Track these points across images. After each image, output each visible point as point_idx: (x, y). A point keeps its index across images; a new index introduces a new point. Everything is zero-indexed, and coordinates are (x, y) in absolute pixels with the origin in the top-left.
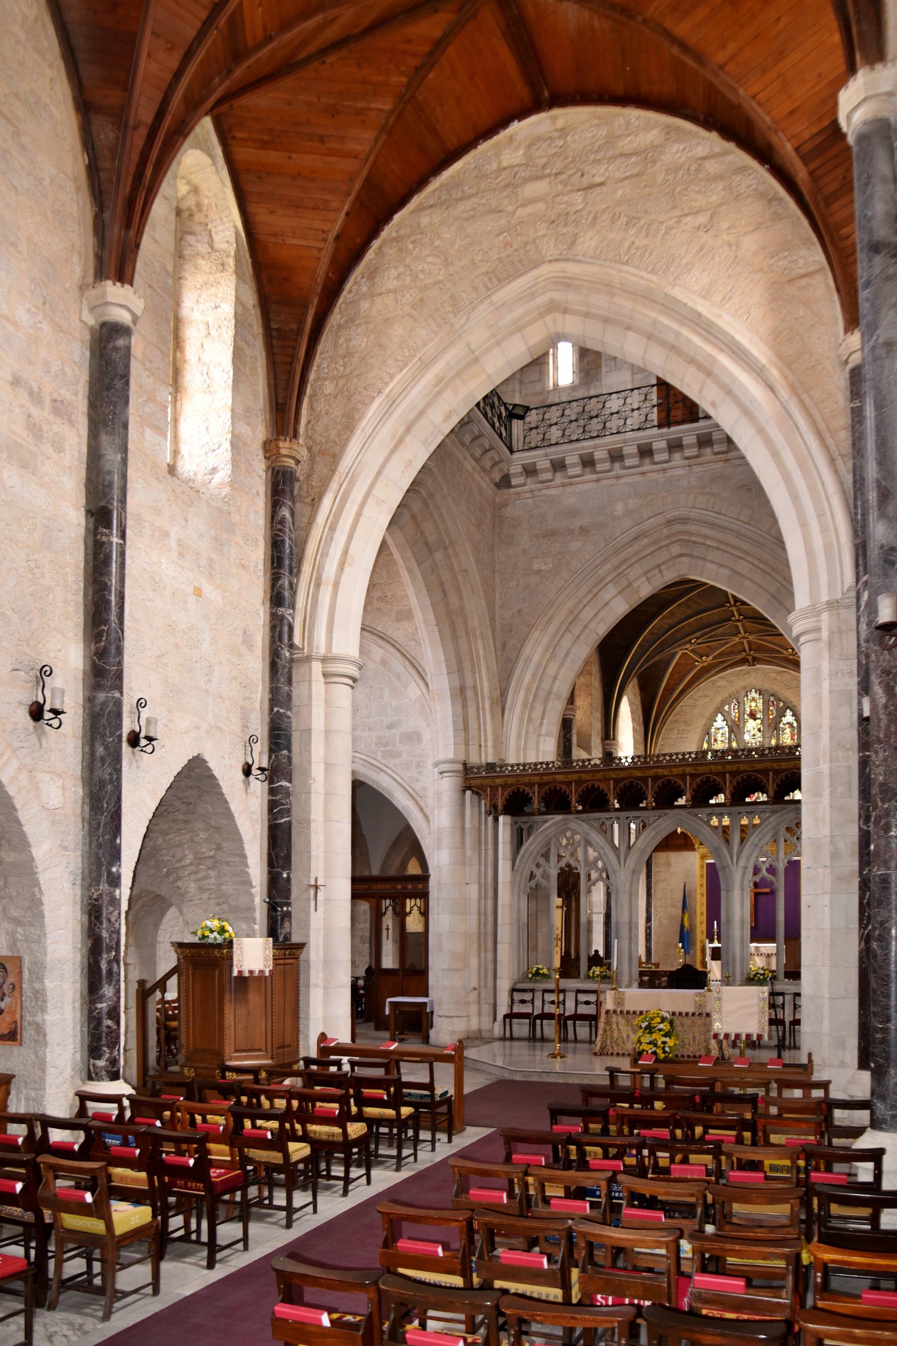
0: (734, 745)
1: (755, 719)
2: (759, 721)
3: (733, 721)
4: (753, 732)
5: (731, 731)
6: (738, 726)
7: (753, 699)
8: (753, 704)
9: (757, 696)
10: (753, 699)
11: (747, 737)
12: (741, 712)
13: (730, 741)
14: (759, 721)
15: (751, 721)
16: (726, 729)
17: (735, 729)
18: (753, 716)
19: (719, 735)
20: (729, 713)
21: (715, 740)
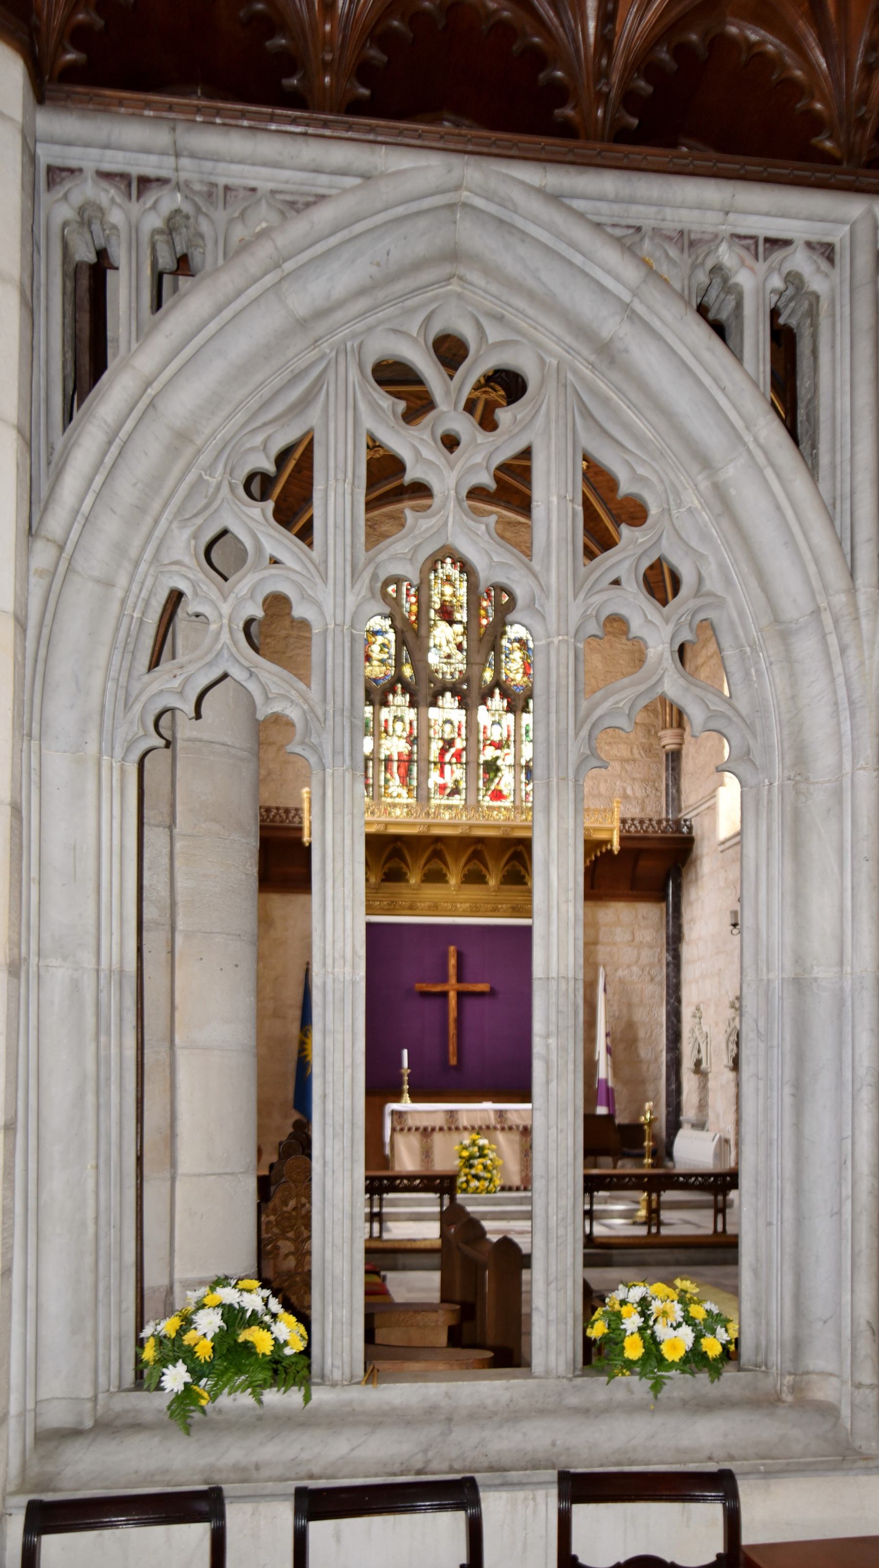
0: (408, 671)
1: (451, 622)
2: (459, 628)
3: (406, 621)
4: (446, 650)
5: (401, 642)
6: (417, 634)
7: (448, 580)
8: (448, 590)
9: (455, 573)
10: (448, 580)
11: (433, 659)
12: (423, 603)
13: (398, 665)
14: (459, 628)
15: (443, 625)
16: (391, 636)
17: (410, 637)
18: (447, 614)
19: (376, 648)
20: (397, 601)
21: (368, 658)
